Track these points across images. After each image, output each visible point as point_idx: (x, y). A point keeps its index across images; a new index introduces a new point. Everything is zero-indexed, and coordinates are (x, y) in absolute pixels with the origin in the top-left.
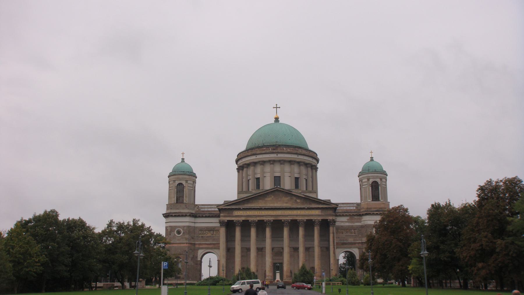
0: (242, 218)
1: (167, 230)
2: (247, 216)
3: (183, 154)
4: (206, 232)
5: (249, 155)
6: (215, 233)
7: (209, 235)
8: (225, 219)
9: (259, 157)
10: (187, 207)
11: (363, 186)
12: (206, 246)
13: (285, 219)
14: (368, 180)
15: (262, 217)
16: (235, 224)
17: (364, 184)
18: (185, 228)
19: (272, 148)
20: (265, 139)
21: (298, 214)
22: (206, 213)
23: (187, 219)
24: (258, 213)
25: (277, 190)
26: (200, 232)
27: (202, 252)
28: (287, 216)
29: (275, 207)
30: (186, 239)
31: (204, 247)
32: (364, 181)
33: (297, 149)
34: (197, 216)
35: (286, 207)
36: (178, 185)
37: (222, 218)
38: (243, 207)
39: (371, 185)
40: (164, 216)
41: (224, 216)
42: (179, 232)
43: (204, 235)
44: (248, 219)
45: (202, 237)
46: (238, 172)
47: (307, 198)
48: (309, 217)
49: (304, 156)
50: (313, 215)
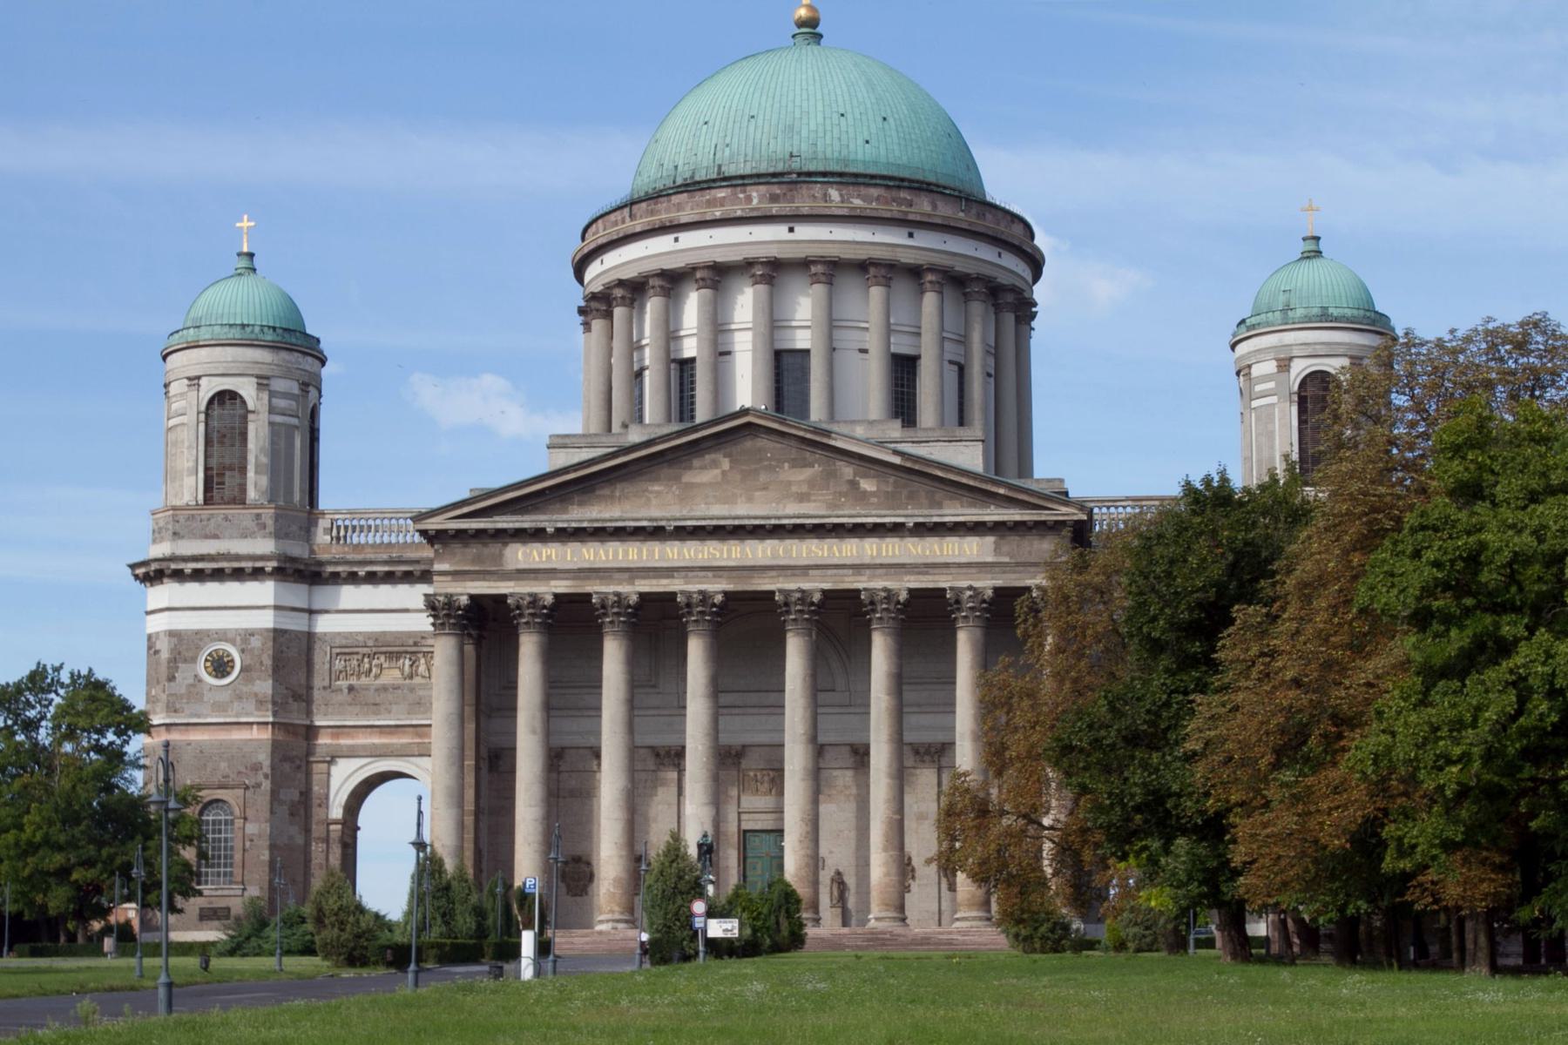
0: (553, 583)
1: (157, 652)
2: (580, 570)
5: (638, 229)
7: (391, 676)
8: (459, 590)
9: (691, 239)
11: (1255, 404)
12: (377, 740)
13: (791, 585)
14: (1284, 365)
15: (668, 577)
16: (599, 617)
17: (1258, 388)
18: (256, 642)
19: (763, 188)
20: (728, 140)
21: (867, 561)
22: (371, 556)
23: (264, 591)
24: (640, 552)
25: (749, 425)
26: (339, 664)
28: (804, 570)
29: (737, 522)
30: (260, 703)
31: (364, 747)
32: (1257, 371)
33: (904, 194)
34: (325, 575)
35: (798, 521)
36: (211, 402)
37: (442, 587)
38: (560, 525)
39: (1296, 399)
40: (136, 577)
41: (457, 575)
42: (220, 666)
43: (364, 680)
44: (588, 589)
45: (351, 689)
46: (587, 326)
47: (917, 467)
48: (927, 573)
49: (947, 237)
50: (947, 565)
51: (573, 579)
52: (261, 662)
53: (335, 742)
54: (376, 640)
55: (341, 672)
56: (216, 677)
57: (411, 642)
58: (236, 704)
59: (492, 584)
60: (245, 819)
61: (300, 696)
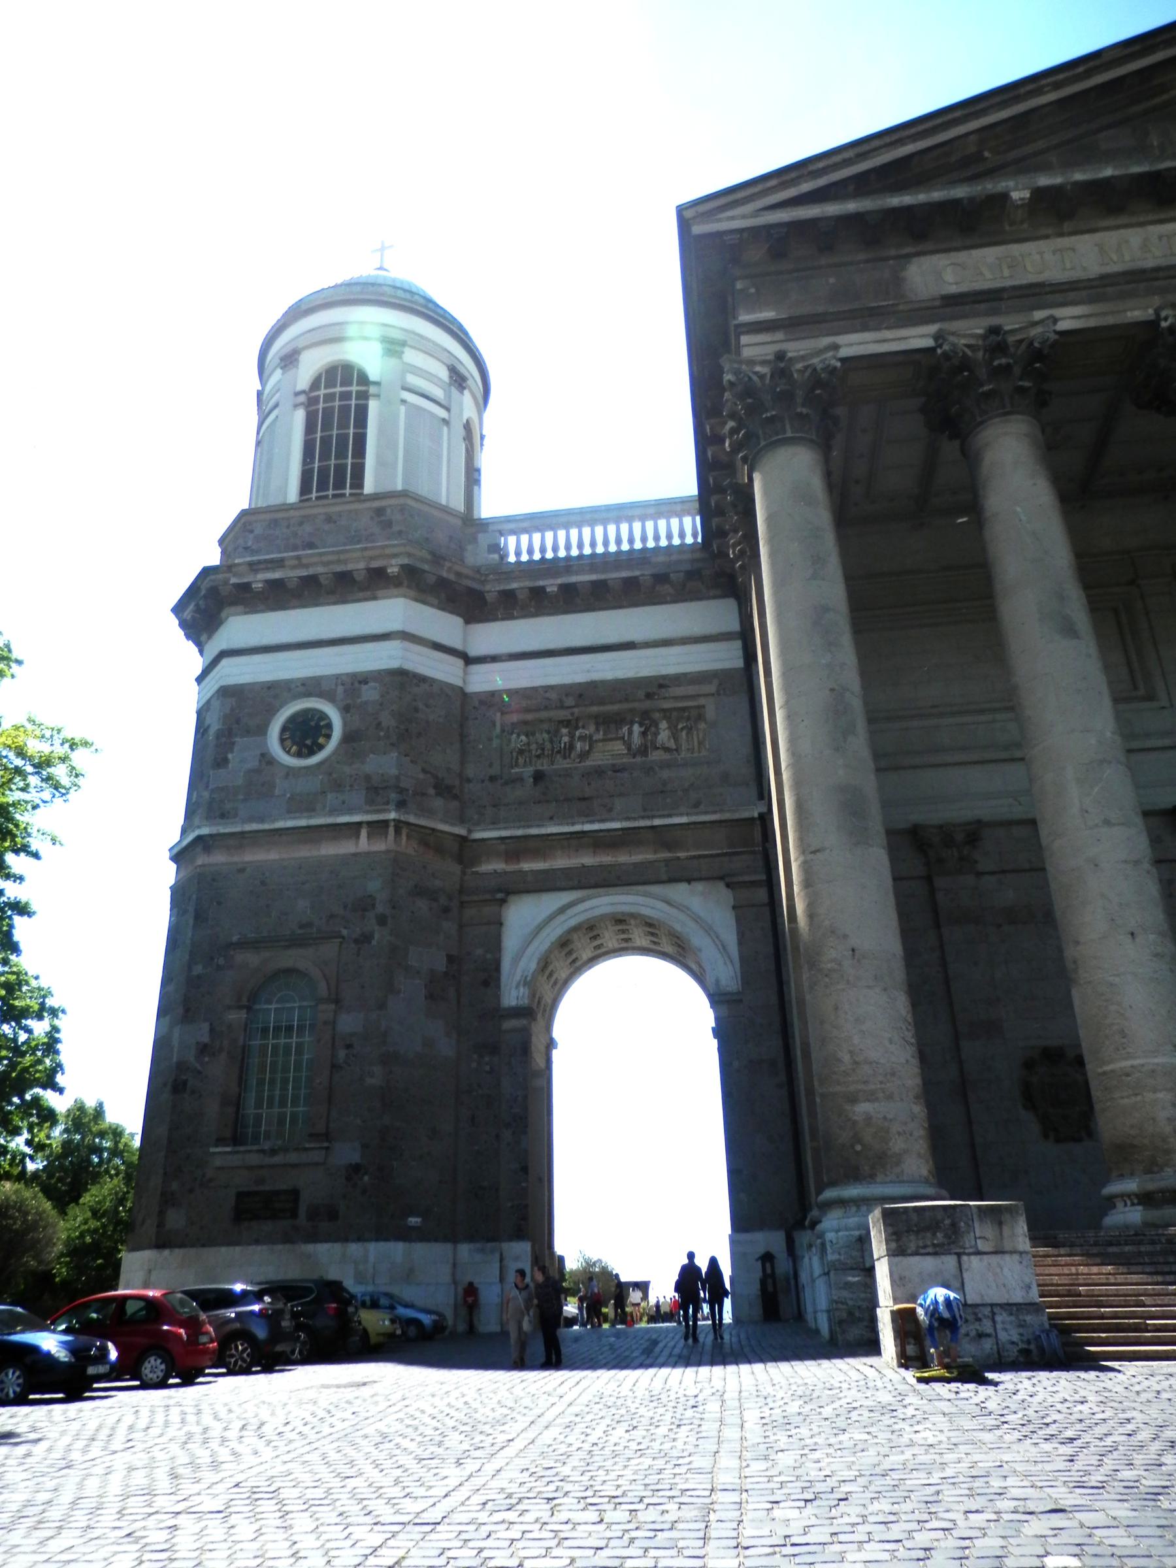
2: (1105, 280)
3: (382, 249)
4: (577, 733)
6: (664, 736)
7: (610, 752)
10: (388, 524)
12: (588, 860)
18: (370, 694)
27: (551, 918)
30: (375, 791)
31: (566, 872)
34: (490, 598)
38: (1044, 181)
41: (792, 325)
43: (561, 764)
45: (538, 777)
51: (1091, 301)
52: (379, 724)
53: (510, 868)
54: (580, 696)
55: (521, 752)
56: (299, 755)
57: (641, 694)
58: (330, 796)
59: (888, 334)
60: (337, 1001)
61: (449, 789)
